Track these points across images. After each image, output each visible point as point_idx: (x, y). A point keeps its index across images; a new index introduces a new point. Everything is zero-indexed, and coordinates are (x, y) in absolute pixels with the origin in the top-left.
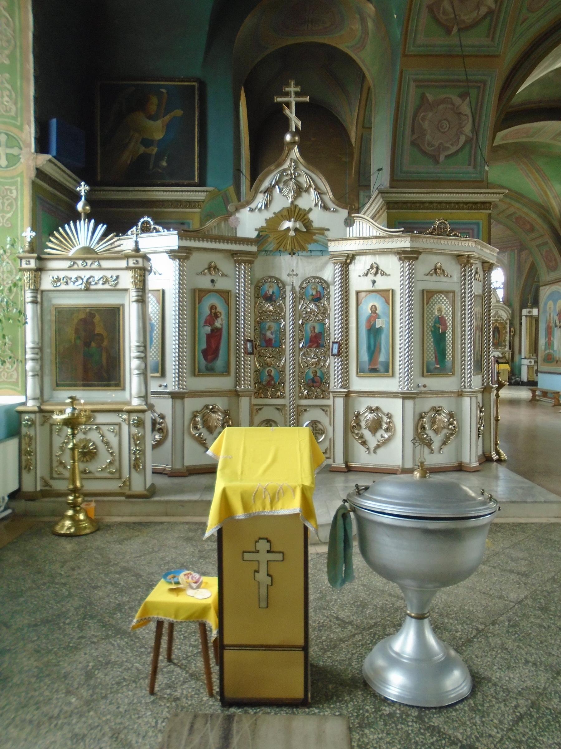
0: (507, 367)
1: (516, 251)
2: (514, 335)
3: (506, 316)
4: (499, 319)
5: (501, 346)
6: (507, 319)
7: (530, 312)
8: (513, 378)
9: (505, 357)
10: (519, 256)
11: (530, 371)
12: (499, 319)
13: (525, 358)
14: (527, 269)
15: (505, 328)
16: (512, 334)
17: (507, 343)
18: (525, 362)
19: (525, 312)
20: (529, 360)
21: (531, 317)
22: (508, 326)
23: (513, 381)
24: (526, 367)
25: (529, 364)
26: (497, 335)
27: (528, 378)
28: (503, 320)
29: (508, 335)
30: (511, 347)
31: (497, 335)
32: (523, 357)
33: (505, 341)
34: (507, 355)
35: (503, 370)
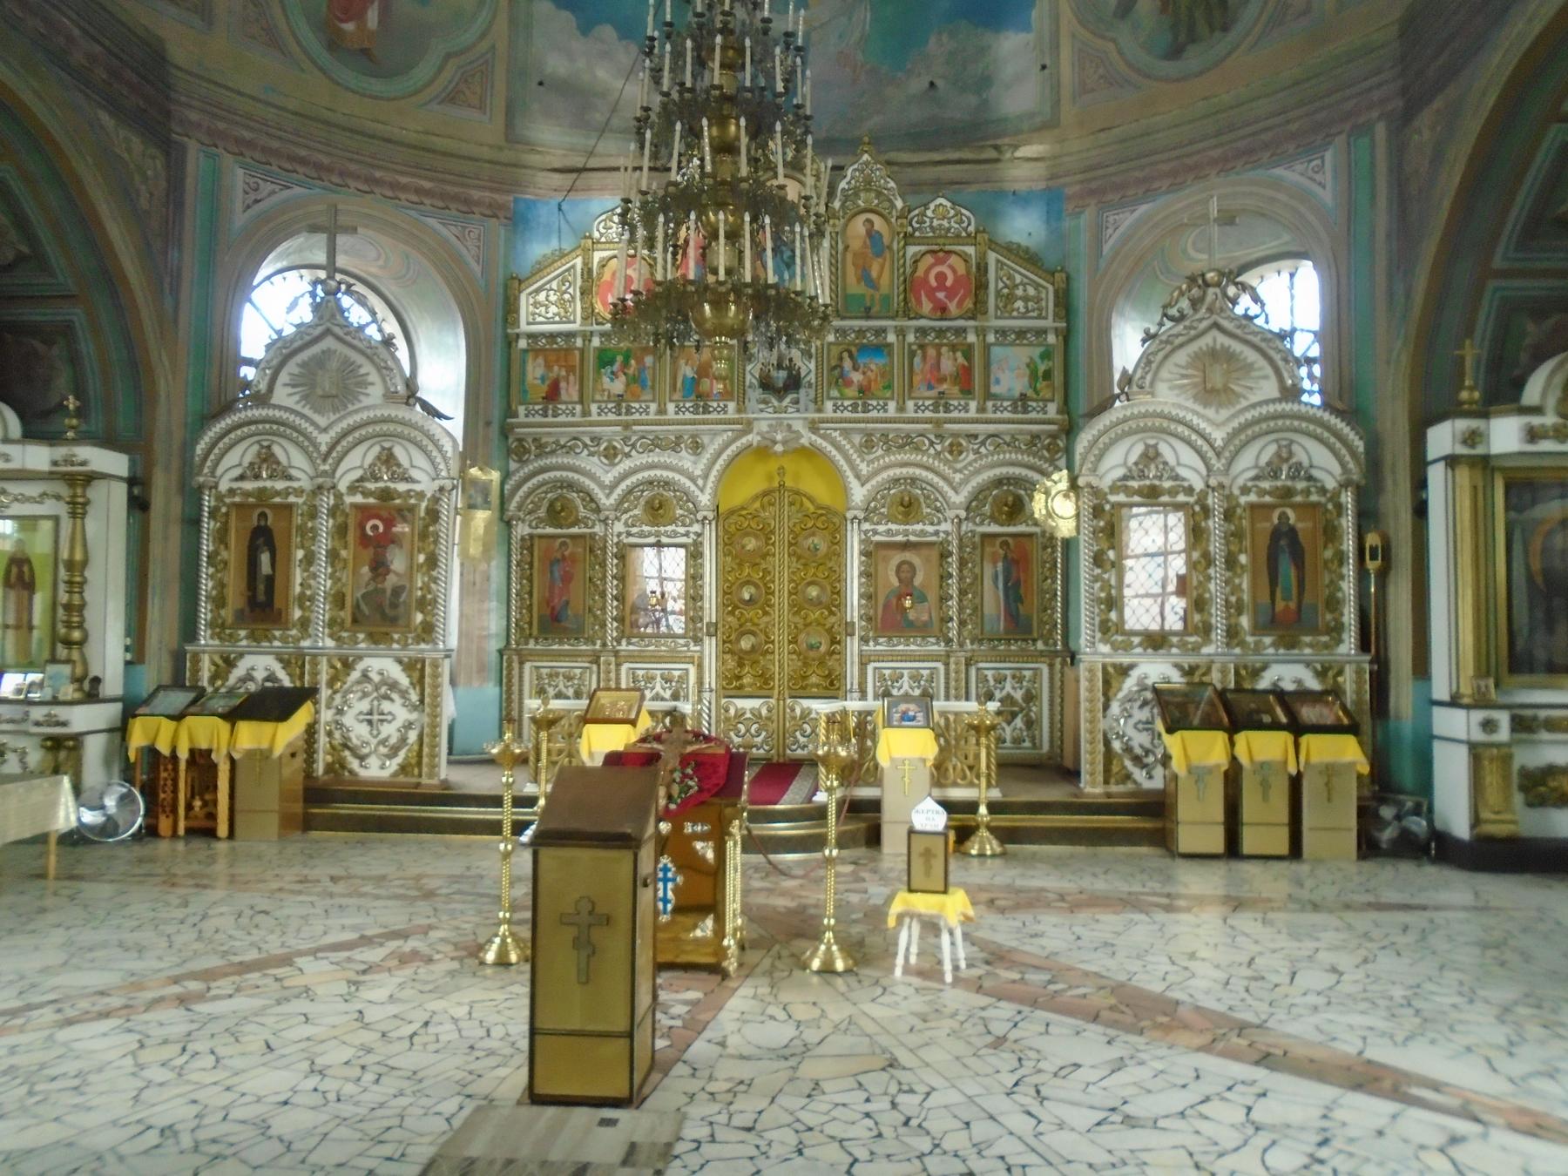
0: (1348, 752)
1: (1381, 130)
2: (1383, 575)
3: (1336, 469)
4: (1300, 485)
5: (1315, 631)
6: (1345, 485)
7: (1472, 438)
8: (1387, 812)
9: (1336, 692)
10: (1398, 150)
11: (1492, 779)
12: (1300, 485)
13: (1454, 702)
14: (1447, 204)
15: (1331, 533)
16: (1372, 566)
17: (1350, 616)
18: (1455, 724)
19: (1442, 438)
20: (1478, 716)
21: (1485, 464)
22: (1348, 523)
23: (1387, 835)
24: (1462, 753)
25: (1478, 736)
26: (1288, 570)
27: (1476, 821)
28: (1323, 491)
29: (1350, 570)
30: (1371, 636)
31: (1288, 570)
32: (1440, 690)
33: (1334, 604)
34: (1348, 681)
35: (1331, 771)
